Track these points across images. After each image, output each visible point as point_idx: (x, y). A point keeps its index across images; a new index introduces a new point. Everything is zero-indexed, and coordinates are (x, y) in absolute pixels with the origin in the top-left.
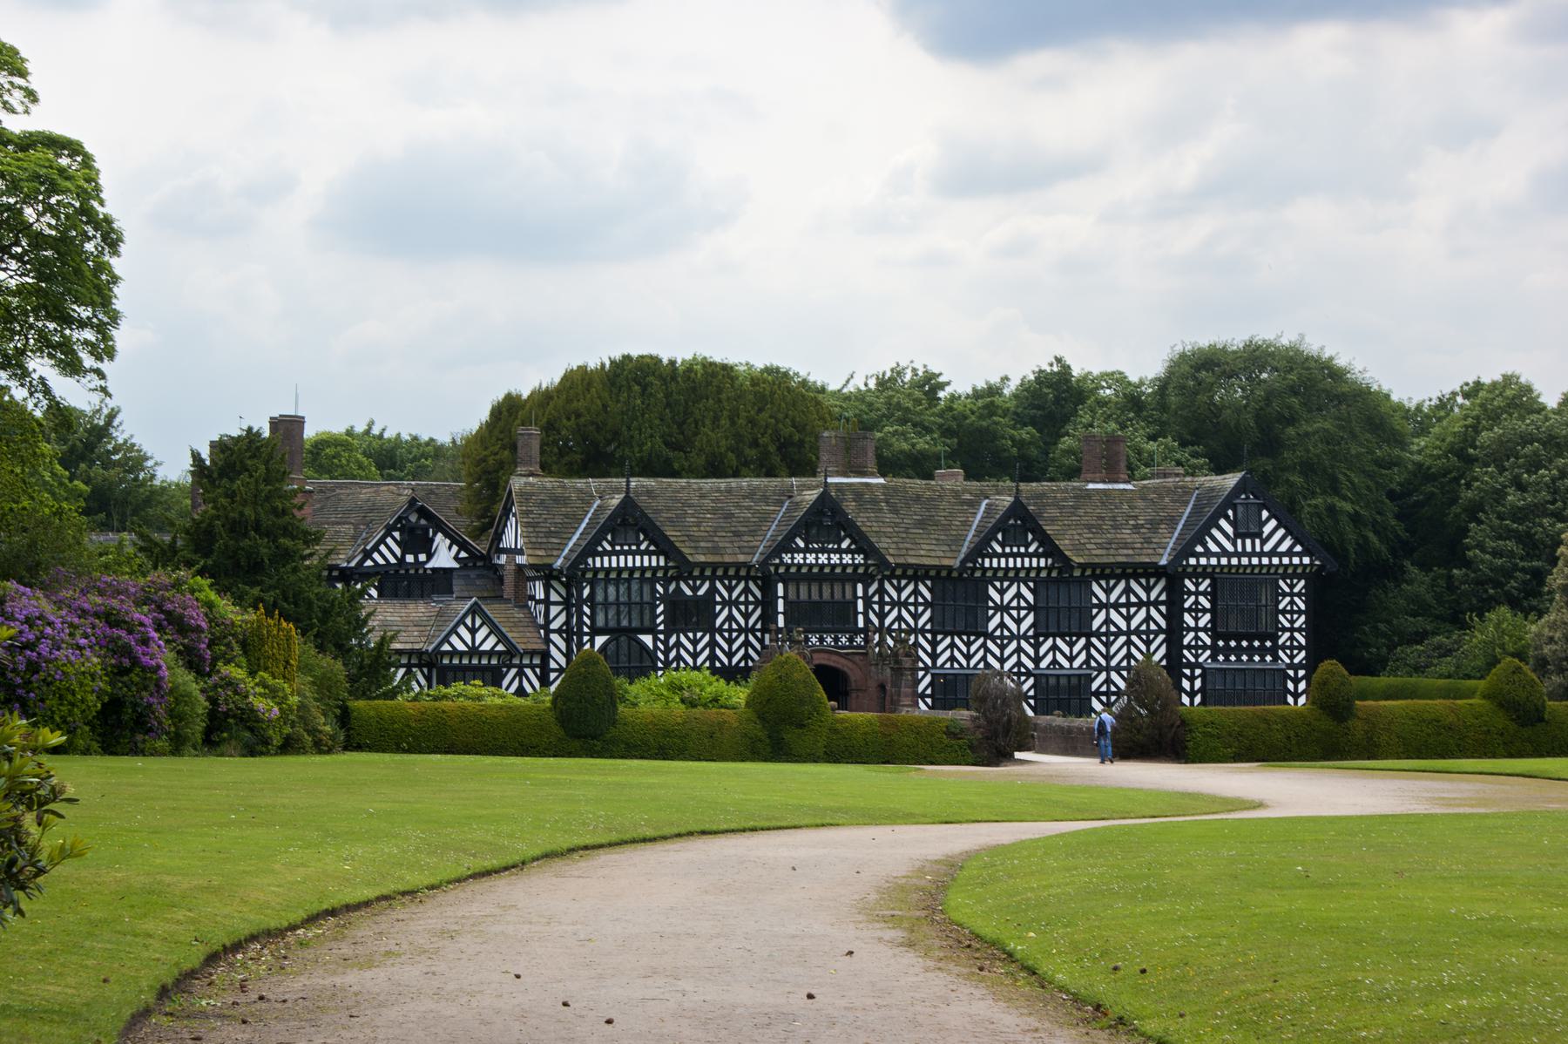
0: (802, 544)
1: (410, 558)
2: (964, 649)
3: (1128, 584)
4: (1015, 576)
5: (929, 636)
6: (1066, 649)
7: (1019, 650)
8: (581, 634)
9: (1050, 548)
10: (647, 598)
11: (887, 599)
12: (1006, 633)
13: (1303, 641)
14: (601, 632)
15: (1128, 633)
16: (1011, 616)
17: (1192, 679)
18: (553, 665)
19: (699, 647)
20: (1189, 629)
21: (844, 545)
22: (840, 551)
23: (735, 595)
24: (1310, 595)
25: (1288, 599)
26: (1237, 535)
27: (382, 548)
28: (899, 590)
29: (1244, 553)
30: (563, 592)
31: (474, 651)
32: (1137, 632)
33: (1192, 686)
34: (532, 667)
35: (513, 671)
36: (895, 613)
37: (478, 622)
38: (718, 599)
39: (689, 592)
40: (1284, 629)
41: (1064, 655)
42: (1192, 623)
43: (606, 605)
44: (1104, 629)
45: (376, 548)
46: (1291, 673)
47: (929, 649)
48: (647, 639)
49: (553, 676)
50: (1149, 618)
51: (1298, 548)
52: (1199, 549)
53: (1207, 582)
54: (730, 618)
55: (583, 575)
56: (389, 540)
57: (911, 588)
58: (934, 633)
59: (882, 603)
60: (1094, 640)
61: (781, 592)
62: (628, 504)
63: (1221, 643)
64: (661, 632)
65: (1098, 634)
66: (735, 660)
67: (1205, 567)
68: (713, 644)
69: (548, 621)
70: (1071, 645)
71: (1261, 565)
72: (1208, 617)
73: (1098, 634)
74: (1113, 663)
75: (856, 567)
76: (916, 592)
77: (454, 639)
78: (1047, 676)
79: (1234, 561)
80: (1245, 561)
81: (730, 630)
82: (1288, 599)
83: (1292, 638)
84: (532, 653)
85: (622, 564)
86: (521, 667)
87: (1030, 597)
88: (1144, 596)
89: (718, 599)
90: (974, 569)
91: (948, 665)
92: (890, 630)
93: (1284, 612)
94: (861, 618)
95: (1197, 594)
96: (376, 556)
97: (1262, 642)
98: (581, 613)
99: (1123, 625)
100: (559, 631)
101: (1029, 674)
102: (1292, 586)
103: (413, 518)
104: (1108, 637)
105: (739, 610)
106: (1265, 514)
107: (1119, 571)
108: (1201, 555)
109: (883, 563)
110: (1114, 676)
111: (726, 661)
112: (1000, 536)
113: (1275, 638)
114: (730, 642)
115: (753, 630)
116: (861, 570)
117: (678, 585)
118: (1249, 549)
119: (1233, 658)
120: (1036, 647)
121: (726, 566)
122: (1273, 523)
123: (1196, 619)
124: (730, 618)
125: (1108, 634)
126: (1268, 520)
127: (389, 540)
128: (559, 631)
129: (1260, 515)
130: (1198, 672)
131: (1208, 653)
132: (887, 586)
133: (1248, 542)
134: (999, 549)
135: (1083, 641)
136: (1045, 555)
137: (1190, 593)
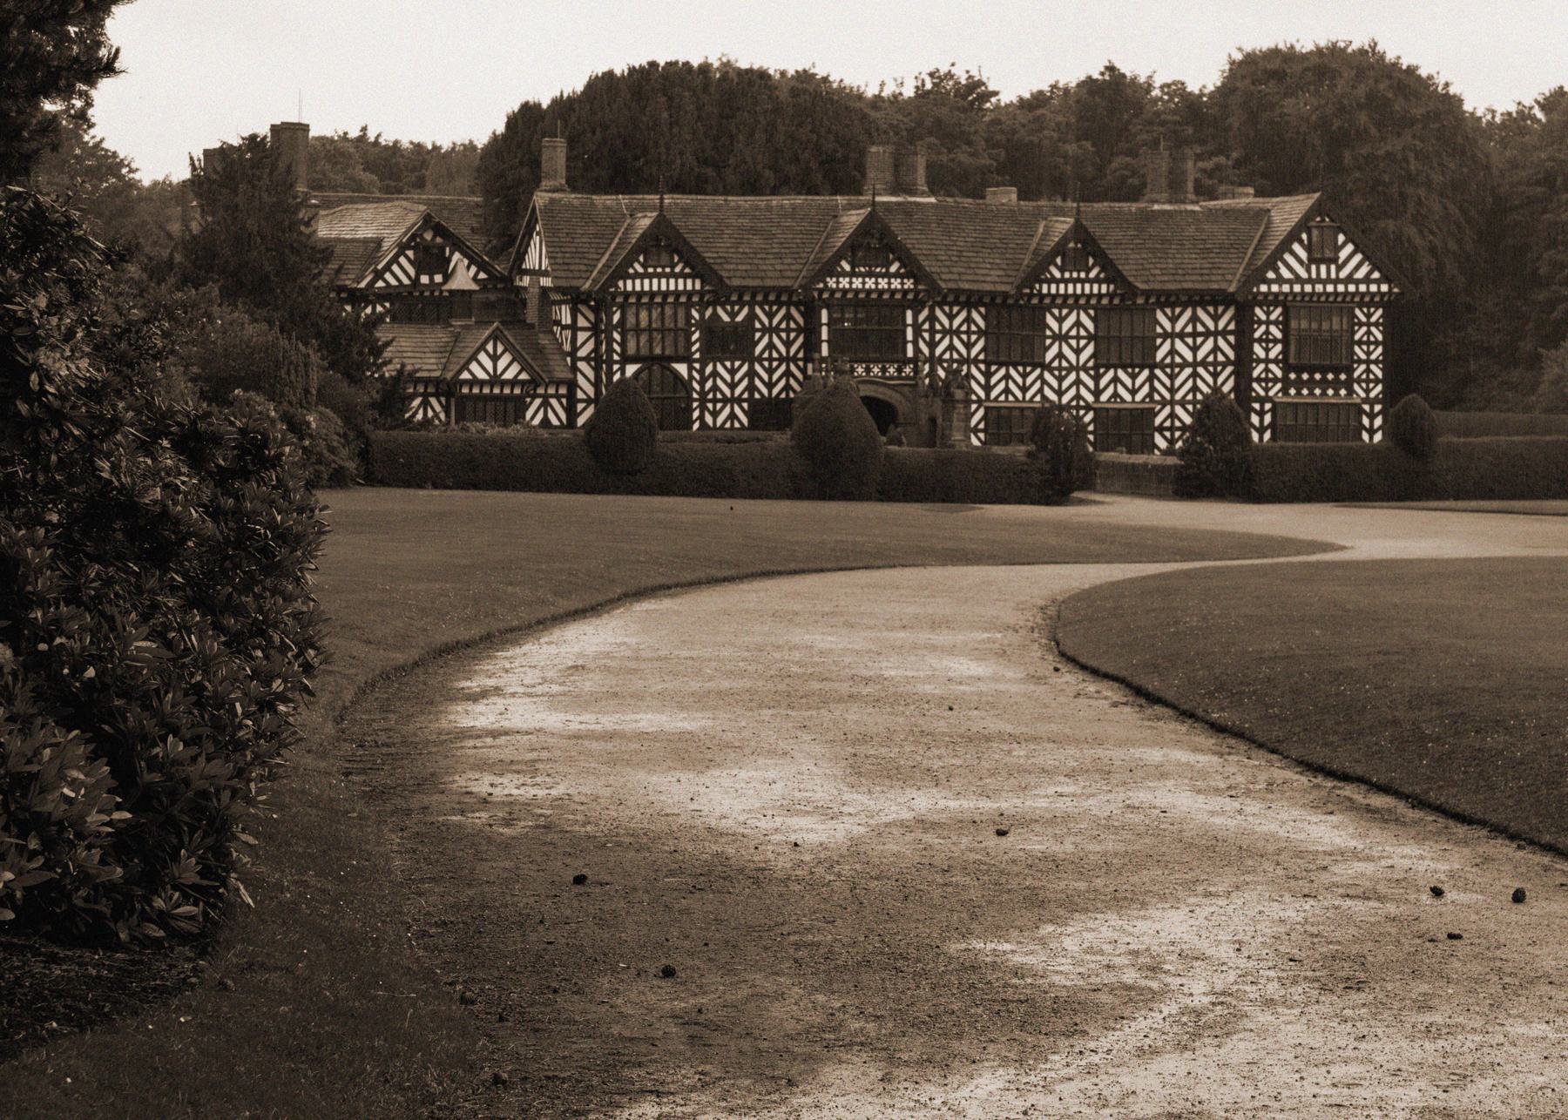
1: (425, 279)
2: (1020, 380)
3: (1194, 313)
4: (1075, 302)
5: (982, 367)
6: (1128, 382)
7: (1078, 382)
8: (610, 362)
10: (681, 324)
11: (938, 327)
12: (1064, 364)
14: (634, 360)
15: (1195, 364)
16: (1070, 346)
17: (1261, 414)
18: (580, 395)
19: (737, 377)
20: (1259, 361)
21: (893, 269)
22: (887, 275)
23: (775, 322)
24: (1389, 325)
25: (1364, 329)
26: (1311, 260)
27: (395, 268)
28: (951, 317)
29: (1319, 280)
31: (495, 380)
32: (1204, 363)
33: (1262, 421)
34: (558, 397)
35: (538, 401)
36: (946, 342)
37: (500, 349)
38: (758, 325)
39: (726, 318)
40: (1360, 361)
41: (1126, 388)
43: (638, 331)
44: (1168, 361)
45: (388, 268)
46: (1366, 407)
47: (982, 380)
48: (682, 368)
49: (580, 406)
51: (1376, 275)
52: (1271, 275)
53: (1279, 310)
54: (771, 346)
55: (614, 298)
56: (402, 260)
57: (964, 314)
58: (988, 363)
59: (932, 331)
60: (1158, 372)
61: (824, 319)
62: (661, 223)
63: (1293, 376)
64: (696, 361)
65: (1162, 366)
66: (775, 391)
67: (1276, 295)
68: (752, 374)
69: (575, 349)
70: (1134, 377)
71: (1336, 294)
72: (1279, 347)
74: (1178, 396)
75: (905, 292)
76: (968, 320)
78: (1107, 410)
79: (1308, 288)
80: (1319, 288)
81: (771, 359)
82: (1364, 329)
83: (1368, 371)
85: (655, 288)
86: (546, 397)
87: (1090, 325)
89: (758, 325)
90: (1031, 296)
91: (1002, 398)
92: (940, 360)
93: (1360, 343)
94: (910, 347)
95: (1267, 324)
96: (388, 276)
97: (1337, 374)
98: (610, 340)
99: (1189, 356)
100: (586, 359)
101: (1088, 408)
102: (1369, 316)
103: (428, 236)
104: (1173, 369)
105: (780, 338)
106: (1341, 238)
107: (1184, 298)
109: (934, 288)
110: (1179, 410)
111: (765, 391)
112: (1059, 260)
113: (1350, 370)
114: (770, 371)
115: (795, 359)
118: (1323, 275)
119: (1305, 392)
121: (767, 291)
122: (1350, 248)
123: (1267, 350)
124: (771, 346)
125: (1172, 365)
127: (402, 260)
128: (586, 359)
129: (1336, 239)
130: (1268, 406)
131: (1279, 386)
132: (938, 313)
133: (1323, 268)
134: (1057, 275)
135: (1146, 373)
136: (1107, 281)
137: (1260, 322)
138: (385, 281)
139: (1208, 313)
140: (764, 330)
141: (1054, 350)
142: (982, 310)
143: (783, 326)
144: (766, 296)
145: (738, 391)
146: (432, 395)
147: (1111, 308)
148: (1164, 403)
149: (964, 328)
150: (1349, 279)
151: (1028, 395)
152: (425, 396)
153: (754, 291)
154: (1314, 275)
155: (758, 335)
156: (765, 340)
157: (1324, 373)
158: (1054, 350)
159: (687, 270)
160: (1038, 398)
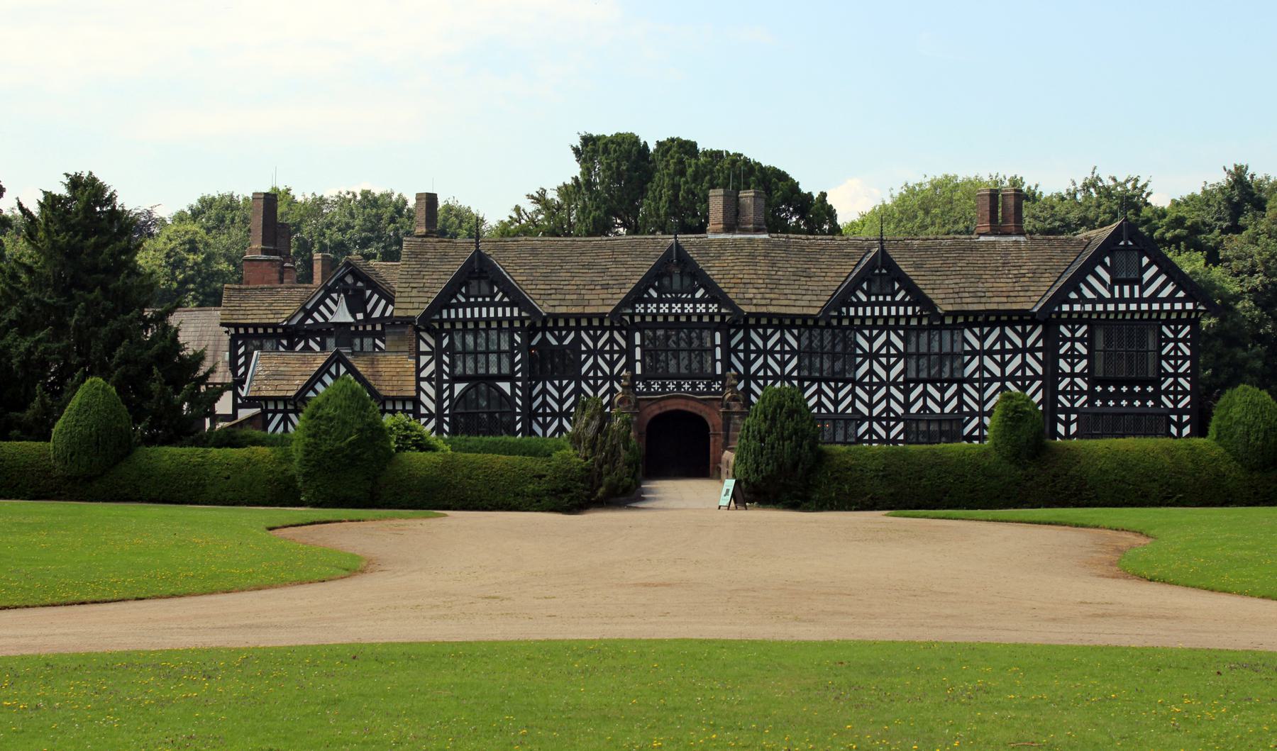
0: (655, 295)
2: (832, 395)
3: (1002, 331)
6: (937, 396)
7: (888, 396)
8: (440, 381)
9: (917, 297)
11: (753, 347)
12: (875, 380)
13: (1188, 386)
15: (1003, 379)
16: (880, 363)
17: (1067, 424)
19: (565, 394)
21: (698, 295)
22: (694, 301)
23: (600, 344)
26: (1114, 281)
27: (322, 308)
28: (765, 338)
29: (1122, 299)
30: (432, 343)
32: (1012, 378)
33: (1067, 430)
37: (343, 370)
38: (583, 348)
39: (554, 342)
40: (1168, 375)
41: (933, 400)
42: (1067, 369)
43: (465, 352)
48: (506, 386)
50: (1024, 364)
52: (1073, 296)
53: (1085, 328)
54: (596, 366)
55: (441, 325)
57: (777, 336)
58: (801, 380)
59: (747, 351)
60: (966, 386)
61: (638, 341)
63: (1099, 389)
64: (519, 379)
65: (970, 380)
70: (942, 391)
72: (1084, 363)
73: (970, 380)
75: (712, 316)
76: (782, 341)
77: (319, 387)
78: (918, 421)
79: (1111, 307)
84: (404, 400)
87: (900, 345)
88: (1019, 342)
89: (583, 348)
90: (840, 318)
92: (755, 378)
93: (1167, 357)
94: (719, 365)
95: (1074, 340)
96: (316, 315)
99: (997, 372)
100: (429, 379)
102: (1176, 332)
105: (604, 359)
107: (992, 318)
108: (1076, 301)
112: (865, 286)
113: (1157, 383)
116: (717, 319)
117: (544, 335)
118: (1127, 295)
120: (907, 393)
121: (590, 317)
122: (1154, 269)
123: (1072, 365)
124: (596, 366)
126: (1149, 266)
128: (429, 379)
129: (1141, 262)
130: (1073, 417)
131: (1085, 398)
133: (1126, 288)
134: (864, 299)
135: (954, 387)
137: (1065, 340)
138: (314, 319)
139: (1016, 332)
140: (590, 352)
141: (866, 366)
142: (795, 332)
143: (607, 348)
144: (590, 322)
145: (565, 407)
146: (291, 411)
147: (920, 328)
148: (972, 414)
149: (778, 348)
150: (1153, 298)
151: (840, 408)
152: (286, 412)
153: (578, 317)
154: (1117, 295)
155: (583, 356)
156: (591, 361)
157: (1118, 387)
158: (866, 366)
159: (506, 299)
160: (849, 411)
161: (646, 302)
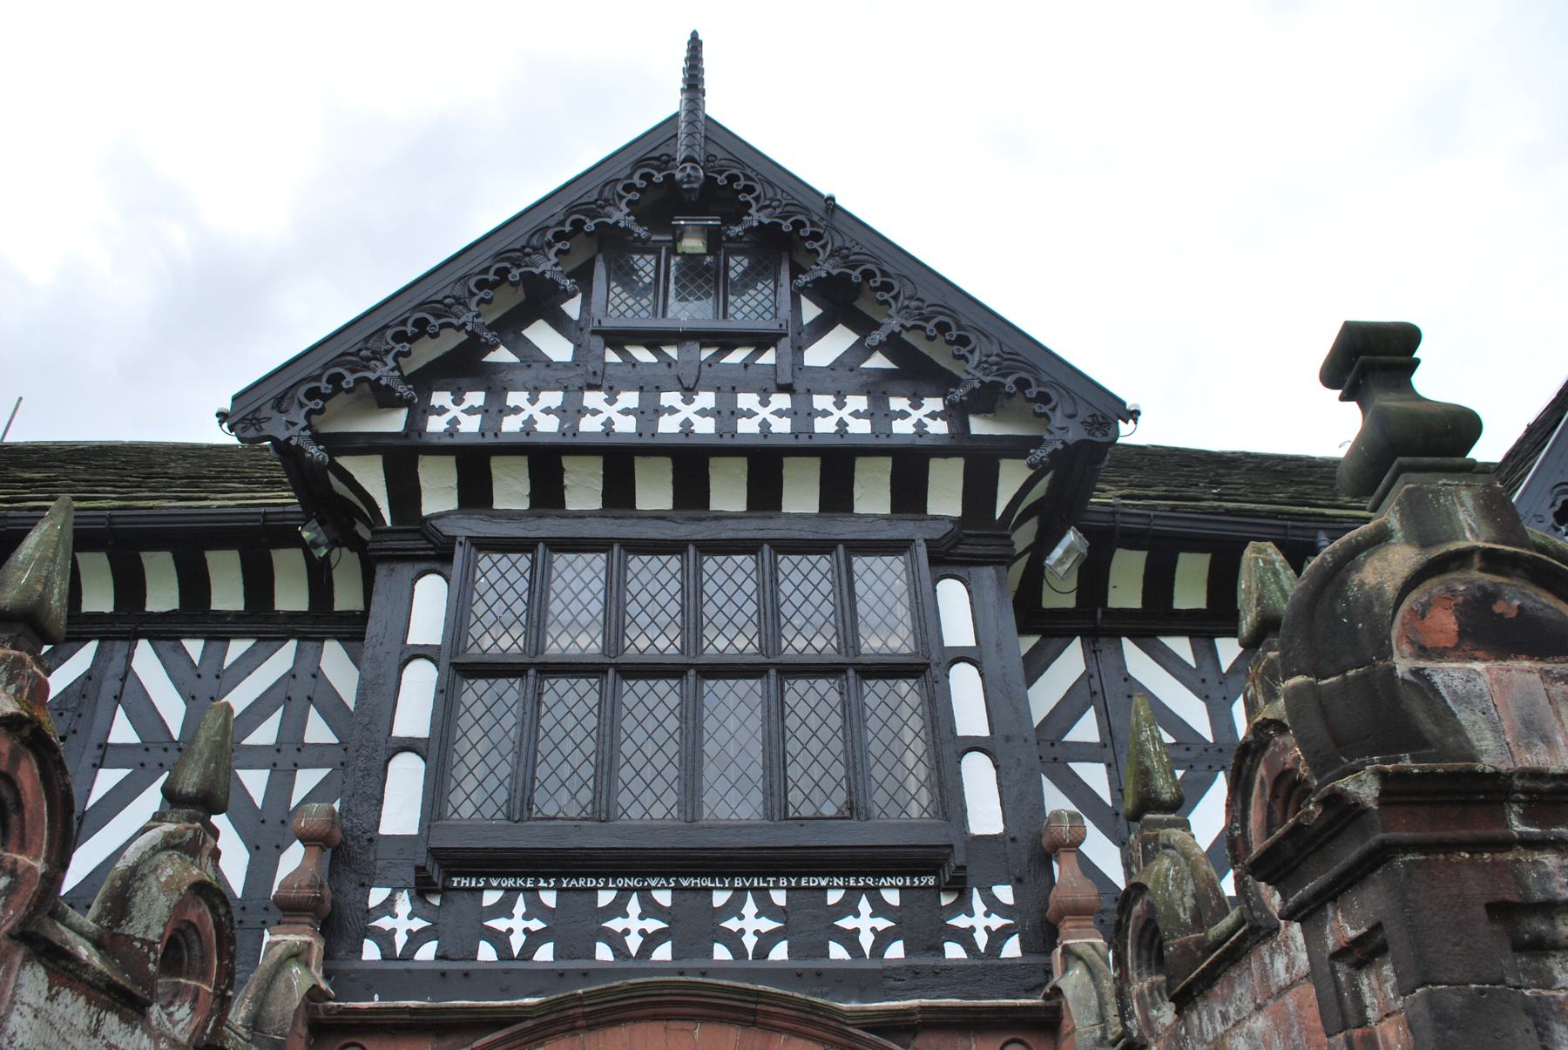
38: (122, 731)
75: (910, 468)
116: (945, 497)
161: (495, 383)
